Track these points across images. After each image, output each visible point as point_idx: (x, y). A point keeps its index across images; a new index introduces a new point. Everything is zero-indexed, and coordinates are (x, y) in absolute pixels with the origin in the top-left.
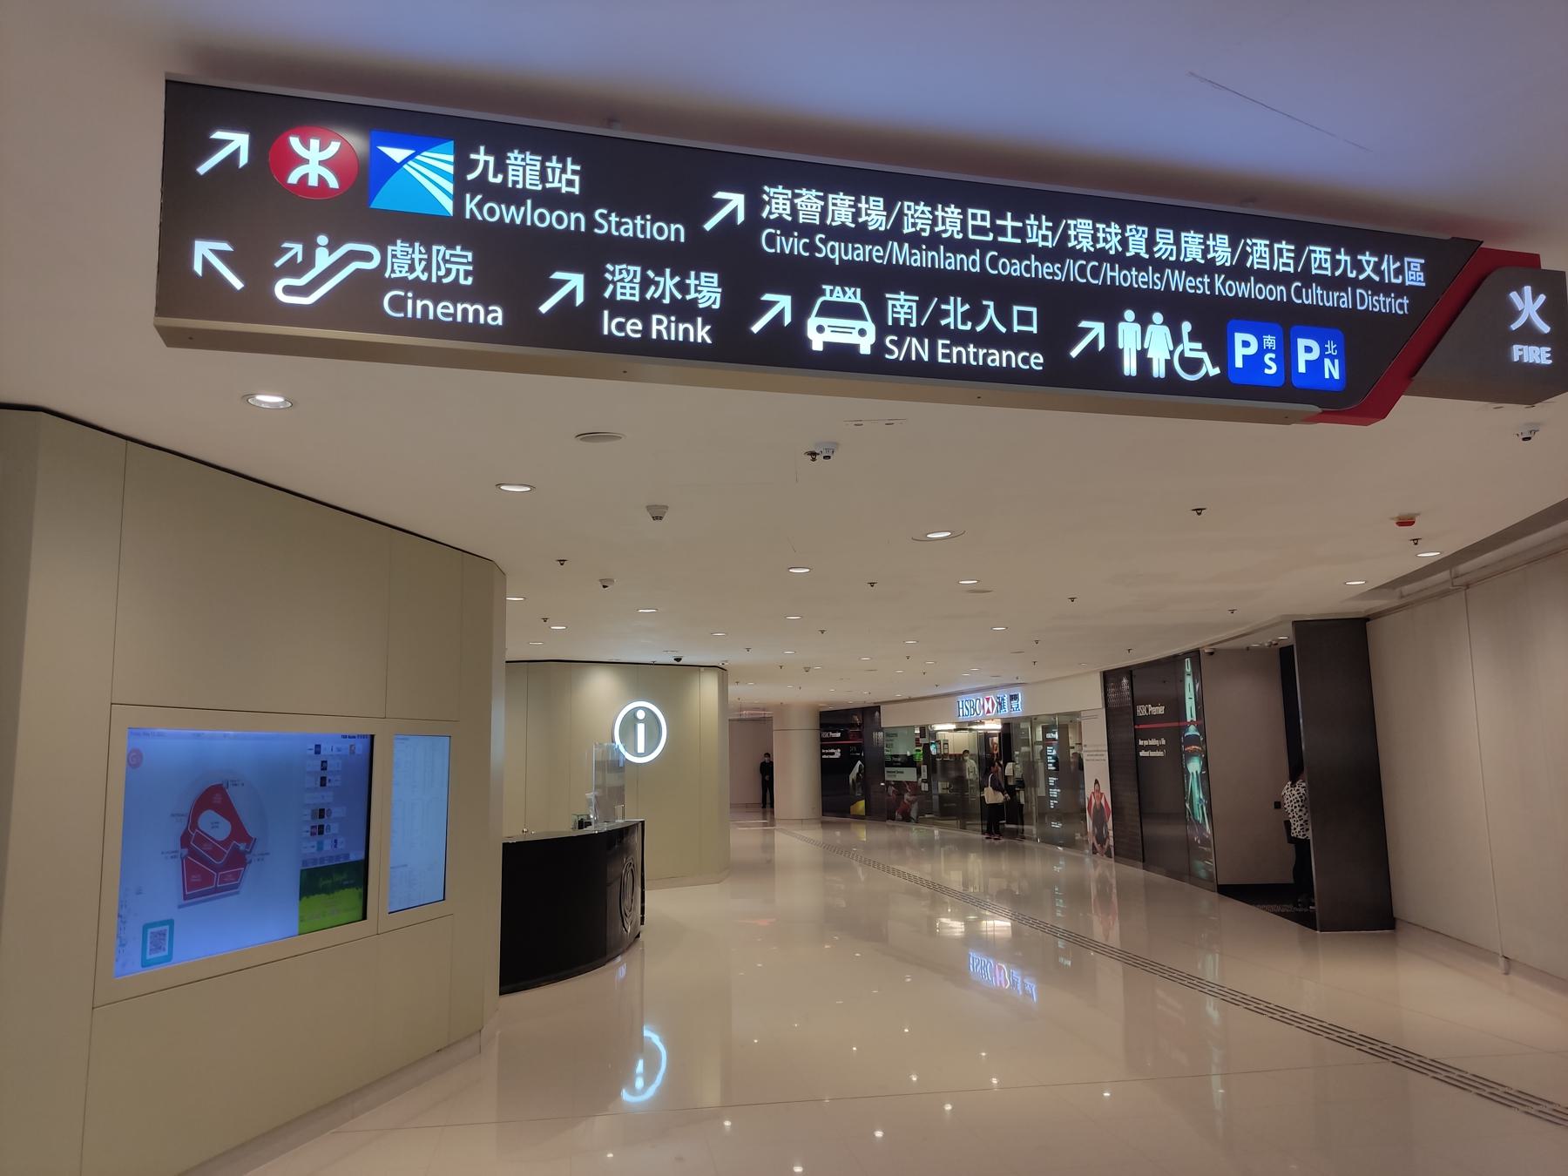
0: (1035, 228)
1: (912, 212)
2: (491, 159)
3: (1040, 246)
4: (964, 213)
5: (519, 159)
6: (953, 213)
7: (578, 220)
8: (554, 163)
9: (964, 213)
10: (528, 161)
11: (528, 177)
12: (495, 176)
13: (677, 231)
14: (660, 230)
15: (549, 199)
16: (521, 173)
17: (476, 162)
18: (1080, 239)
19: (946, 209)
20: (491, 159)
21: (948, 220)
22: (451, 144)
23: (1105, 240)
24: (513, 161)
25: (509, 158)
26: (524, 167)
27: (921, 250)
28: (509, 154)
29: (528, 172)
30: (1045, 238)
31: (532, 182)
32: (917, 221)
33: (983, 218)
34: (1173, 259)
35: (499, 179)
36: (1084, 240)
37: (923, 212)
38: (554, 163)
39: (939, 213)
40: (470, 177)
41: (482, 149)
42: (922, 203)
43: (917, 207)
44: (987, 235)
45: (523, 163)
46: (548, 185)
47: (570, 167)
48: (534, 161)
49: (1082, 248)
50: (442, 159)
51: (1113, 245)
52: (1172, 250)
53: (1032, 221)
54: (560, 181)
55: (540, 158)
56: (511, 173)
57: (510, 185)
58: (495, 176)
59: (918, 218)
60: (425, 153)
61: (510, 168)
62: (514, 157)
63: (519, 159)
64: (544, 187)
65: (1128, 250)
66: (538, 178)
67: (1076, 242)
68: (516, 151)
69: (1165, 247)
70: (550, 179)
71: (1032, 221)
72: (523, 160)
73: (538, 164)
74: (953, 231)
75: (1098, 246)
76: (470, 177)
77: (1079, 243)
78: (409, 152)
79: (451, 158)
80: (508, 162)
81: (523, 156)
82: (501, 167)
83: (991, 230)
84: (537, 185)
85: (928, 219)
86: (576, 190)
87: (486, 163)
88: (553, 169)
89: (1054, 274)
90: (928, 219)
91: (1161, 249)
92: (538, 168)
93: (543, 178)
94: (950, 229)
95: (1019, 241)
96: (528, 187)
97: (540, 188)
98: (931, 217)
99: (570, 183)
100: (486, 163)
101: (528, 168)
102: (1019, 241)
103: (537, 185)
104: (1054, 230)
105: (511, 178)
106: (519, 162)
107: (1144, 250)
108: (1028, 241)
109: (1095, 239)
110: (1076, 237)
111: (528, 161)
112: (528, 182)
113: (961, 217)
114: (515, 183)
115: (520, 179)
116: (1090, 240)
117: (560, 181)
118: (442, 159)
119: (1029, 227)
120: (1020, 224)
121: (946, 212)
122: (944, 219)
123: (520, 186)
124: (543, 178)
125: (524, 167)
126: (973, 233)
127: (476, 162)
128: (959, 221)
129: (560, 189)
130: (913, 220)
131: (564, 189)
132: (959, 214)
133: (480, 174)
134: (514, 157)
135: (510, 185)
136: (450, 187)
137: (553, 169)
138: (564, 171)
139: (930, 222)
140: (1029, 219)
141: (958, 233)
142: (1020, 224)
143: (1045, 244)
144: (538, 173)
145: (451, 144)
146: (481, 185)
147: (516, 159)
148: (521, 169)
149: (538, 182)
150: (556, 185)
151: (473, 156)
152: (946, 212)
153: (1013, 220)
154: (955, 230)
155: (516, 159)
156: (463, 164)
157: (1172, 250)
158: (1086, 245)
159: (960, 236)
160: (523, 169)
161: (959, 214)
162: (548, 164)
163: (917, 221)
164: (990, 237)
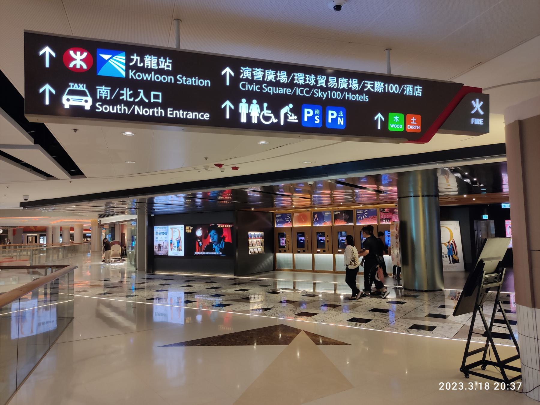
2: (139, 58)
5: (149, 58)
7: (171, 79)
8: (162, 59)
10: (152, 59)
11: (152, 64)
12: (140, 64)
13: (208, 83)
14: (201, 83)
15: (160, 72)
16: (150, 63)
17: (133, 60)
18: (299, 80)
20: (139, 58)
22: (124, 53)
23: (309, 80)
25: (145, 58)
26: (151, 61)
28: (145, 56)
29: (152, 63)
31: (154, 66)
34: (335, 87)
35: (142, 65)
36: (301, 81)
38: (162, 59)
40: (131, 64)
41: (135, 55)
45: (151, 60)
46: (160, 67)
48: (154, 59)
49: (300, 83)
50: (121, 58)
51: (312, 82)
52: (335, 84)
54: (164, 66)
55: (157, 58)
57: (146, 67)
58: (140, 64)
60: (116, 56)
61: (146, 61)
62: (147, 58)
63: (149, 58)
64: (158, 67)
65: (318, 84)
66: (156, 64)
67: (297, 81)
68: (148, 55)
69: (332, 83)
70: (161, 65)
72: (150, 58)
73: (156, 60)
75: (306, 83)
76: (131, 64)
77: (299, 81)
78: (110, 56)
81: (150, 57)
82: (142, 61)
84: (156, 67)
86: (170, 69)
87: (137, 60)
88: (162, 62)
91: (331, 84)
92: (156, 61)
96: (153, 68)
97: (157, 68)
99: (168, 66)
100: (137, 60)
101: (152, 61)
103: (156, 67)
107: (324, 84)
109: (305, 80)
110: (297, 79)
112: (152, 66)
114: (148, 66)
115: (150, 65)
116: (303, 80)
117: (164, 66)
123: (149, 67)
124: (158, 64)
125: (151, 61)
127: (133, 60)
129: (164, 68)
131: (166, 68)
133: (135, 63)
134: (147, 58)
136: (124, 67)
137: (162, 62)
138: (166, 62)
144: (156, 63)
146: (135, 67)
147: (148, 58)
148: (150, 61)
149: (156, 66)
150: (163, 67)
151: (132, 57)
155: (148, 58)
156: (129, 60)
157: (335, 84)
158: (301, 82)
160: (151, 61)
162: (160, 60)
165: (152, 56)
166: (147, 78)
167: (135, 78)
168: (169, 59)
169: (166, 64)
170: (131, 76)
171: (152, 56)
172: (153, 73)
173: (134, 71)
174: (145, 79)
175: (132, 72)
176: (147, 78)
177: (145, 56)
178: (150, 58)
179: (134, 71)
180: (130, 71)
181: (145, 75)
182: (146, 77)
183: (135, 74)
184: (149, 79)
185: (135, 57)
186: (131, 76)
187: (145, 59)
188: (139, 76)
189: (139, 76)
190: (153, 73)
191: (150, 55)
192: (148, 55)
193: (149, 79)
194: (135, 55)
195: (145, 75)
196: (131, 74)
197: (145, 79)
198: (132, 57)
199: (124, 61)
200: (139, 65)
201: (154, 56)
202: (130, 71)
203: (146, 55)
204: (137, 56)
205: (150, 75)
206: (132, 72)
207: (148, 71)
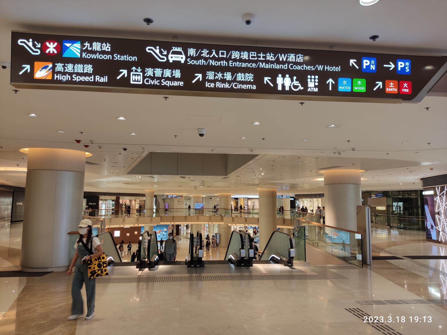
0: (269, 56)
1: (234, 53)
3: (270, 60)
4: (249, 53)
5: (96, 44)
6: (246, 53)
8: (104, 44)
9: (249, 53)
10: (98, 44)
11: (98, 48)
12: (90, 48)
15: (103, 52)
16: (96, 47)
17: (85, 46)
19: (244, 52)
20: (89, 45)
21: (244, 55)
24: (94, 45)
25: (93, 44)
26: (97, 46)
27: (269, 64)
28: (93, 43)
29: (98, 47)
30: (272, 58)
31: (99, 49)
32: (236, 55)
33: (254, 54)
35: (91, 49)
37: (237, 53)
38: (104, 44)
39: (242, 53)
40: (84, 49)
41: (87, 42)
42: (237, 51)
43: (236, 52)
44: (255, 58)
46: (102, 50)
47: (108, 45)
48: (99, 44)
53: (268, 54)
54: (105, 48)
55: (101, 44)
56: (93, 47)
57: (93, 50)
58: (90, 48)
59: (236, 55)
61: (93, 46)
62: (94, 44)
63: (96, 44)
64: (102, 50)
68: (95, 42)
71: (268, 54)
72: (97, 44)
74: (245, 58)
76: (84, 49)
79: (80, 45)
80: (93, 45)
81: (96, 43)
82: (91, 46)
83: (256, 57)
85: (239, 55)
86: (109, 50)
87: (88, 46)
89: (311, 69)
90: (239, 55)
92: (100, 46)
93: (101, 48)
94: (245, 57)
95: (264, 59)
96: (98, 50)
97: (100, 50)
98: (240, 54)
100: (88, 46)
101: (98, 46)
102: (264, 59)
104: (275, 56)
105: (93, 49)
106: (96, 45)
108: (267, 59)
111: (98, 44)
112: (98, 49)
113: (248, 54)
114: (94, 49)
115: (96, 49)
118: (78, 45)
119: (267, 56)
120: (265, 55)
121: (244, 53)
122: (243, 55)
123: (96, 50)
124: (101, 48)
125: (97, 46)
126: (251, 58)
127: (85, 46)
128: (247, 55)
129: (105, 50)
130: (235, 55)
131: (107, 50)
132: (247, 53)
134: (94, 44)
135: (93, 50)
136: (79, 51)
137: (104, 46)
138: (106, 46)
139: (239, 56)
140: (267, 54)
141: (247, 58)
142: (265, 55)
143: (272, 60)
144: (100, 47)
145: (80, 42)
146: (87, 51)
147: (95, 44)
148: (96, 46)
149: (100, 49)
150: (105, 49)
151: (85, 44)
152: (244, 53)
153: (263, 54)
154: (246, 57)
155: (95, 44)
156: (83, 46)
159: (248, 59)
160: (97, 46)
161: (247, 53)
162: (102, 45)
163: (236, 55)
164: (256, 59)
165: (98, 43)
166: (94, 57)
167: (86, 58)
168: (109, 44)
169: (107, 47)
170: (84, 56)
171: (98, 43)
172: (98, 53)
173: (86, 53)
174: (93, 58)
175: (84, 53)
176: (94, 57)
177: (93, 43)
178: (97, 44)
179: (86, 53)
180: (83, 53)
181: (93, 55)
182: (93, 56)
183: (86, 55)
184: (95, 58)
185: (87, 44)
186: (84, 56)
187: (93, 45)
188: (89, 56)
189: (89, 56)
190: (98, 53)
191: (96, 42)
192: (95, 42)
193: (95, 58)
194: (87, 42)
195: (93, 55)
196: (84, 55)
197: (93, 58)
198: (85, 44)
199: (79, 47)
200: (89, 49)
201: (99, 42)
202: (83, 53)
203: (94, 42)
204: (88, 43)
205: (96, 55)
206: (84, 53)
207: (95, 52)
